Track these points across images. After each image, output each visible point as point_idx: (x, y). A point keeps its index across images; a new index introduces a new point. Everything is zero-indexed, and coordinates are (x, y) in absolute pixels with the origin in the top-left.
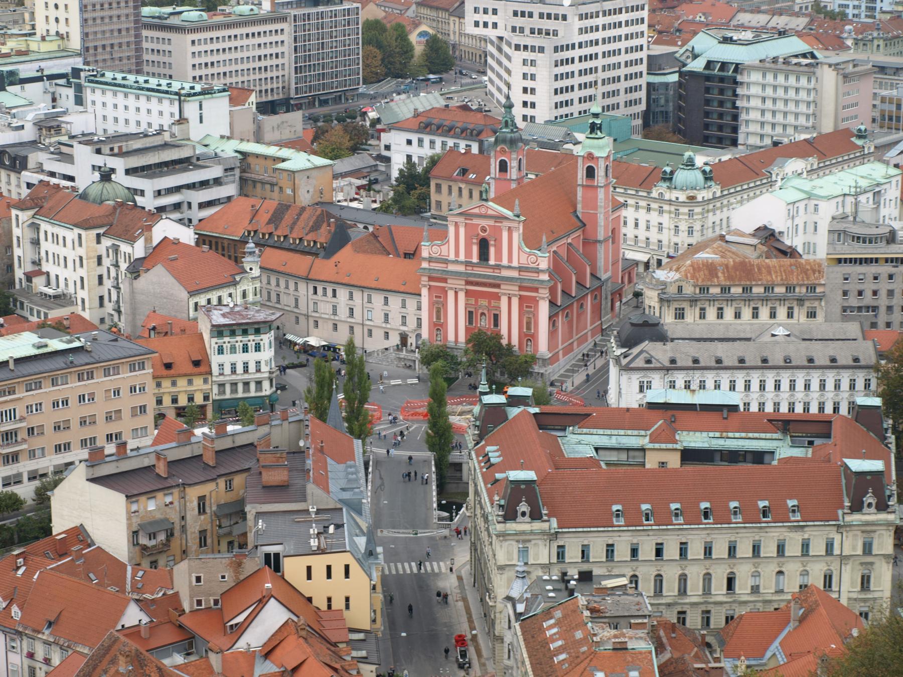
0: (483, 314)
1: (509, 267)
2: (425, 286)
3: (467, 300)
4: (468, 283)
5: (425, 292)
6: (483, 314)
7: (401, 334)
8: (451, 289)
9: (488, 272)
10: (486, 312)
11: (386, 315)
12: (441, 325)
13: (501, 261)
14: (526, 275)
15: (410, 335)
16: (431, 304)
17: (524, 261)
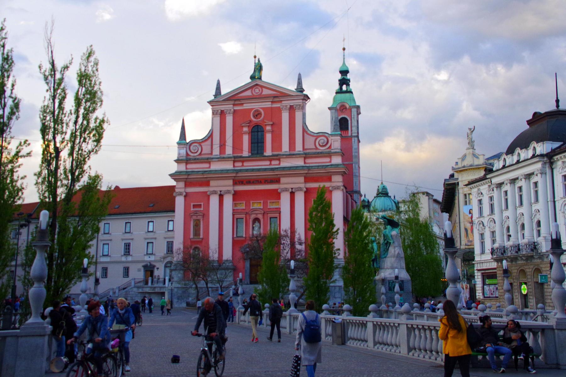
0: (256, 220)
1: (290, 156)
2: (180, 194)
3: (235, 205)
4: (236, 182)
5: (180, 202)
6: (256, 220)
7: (145, 267)
8: (215, 192)
9: (264, 164)
10: (260, 217)
11: (127, 247)
12: (200, 242)
13: (281, 149)
14: (312, 162)
15: (157, 265)
16: (187, 216)
17: (310, 144)
